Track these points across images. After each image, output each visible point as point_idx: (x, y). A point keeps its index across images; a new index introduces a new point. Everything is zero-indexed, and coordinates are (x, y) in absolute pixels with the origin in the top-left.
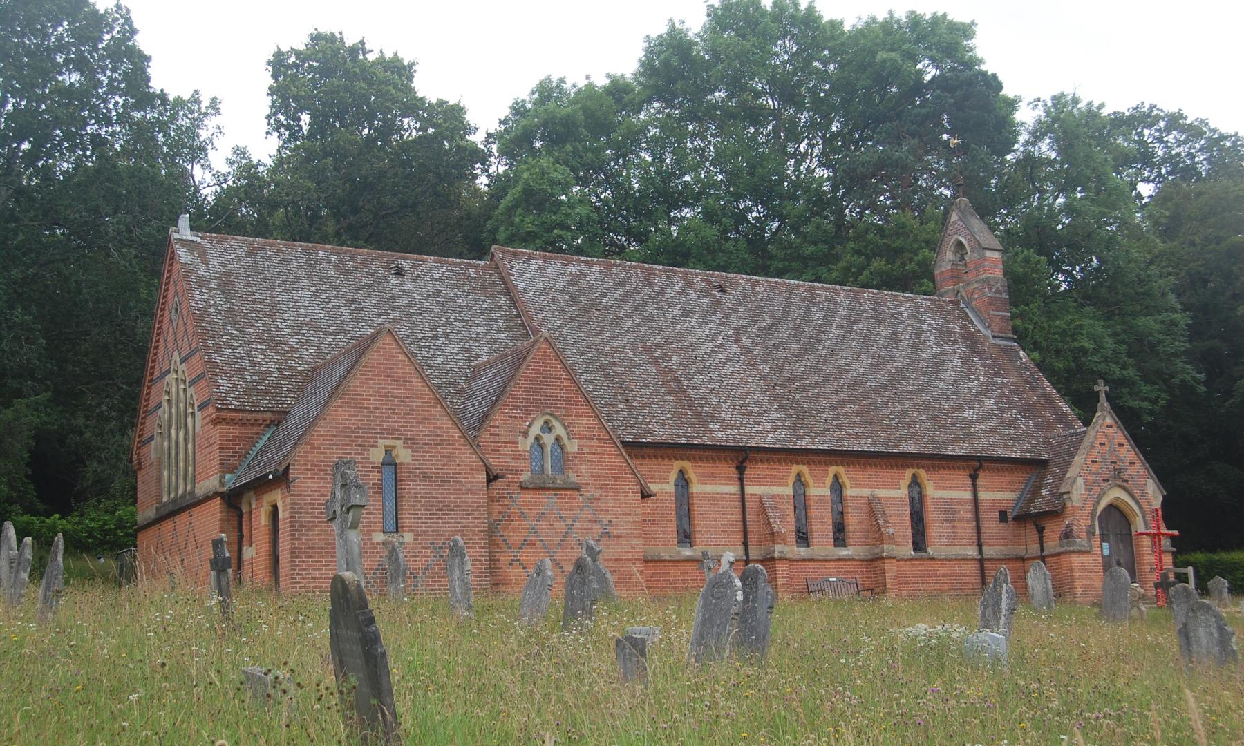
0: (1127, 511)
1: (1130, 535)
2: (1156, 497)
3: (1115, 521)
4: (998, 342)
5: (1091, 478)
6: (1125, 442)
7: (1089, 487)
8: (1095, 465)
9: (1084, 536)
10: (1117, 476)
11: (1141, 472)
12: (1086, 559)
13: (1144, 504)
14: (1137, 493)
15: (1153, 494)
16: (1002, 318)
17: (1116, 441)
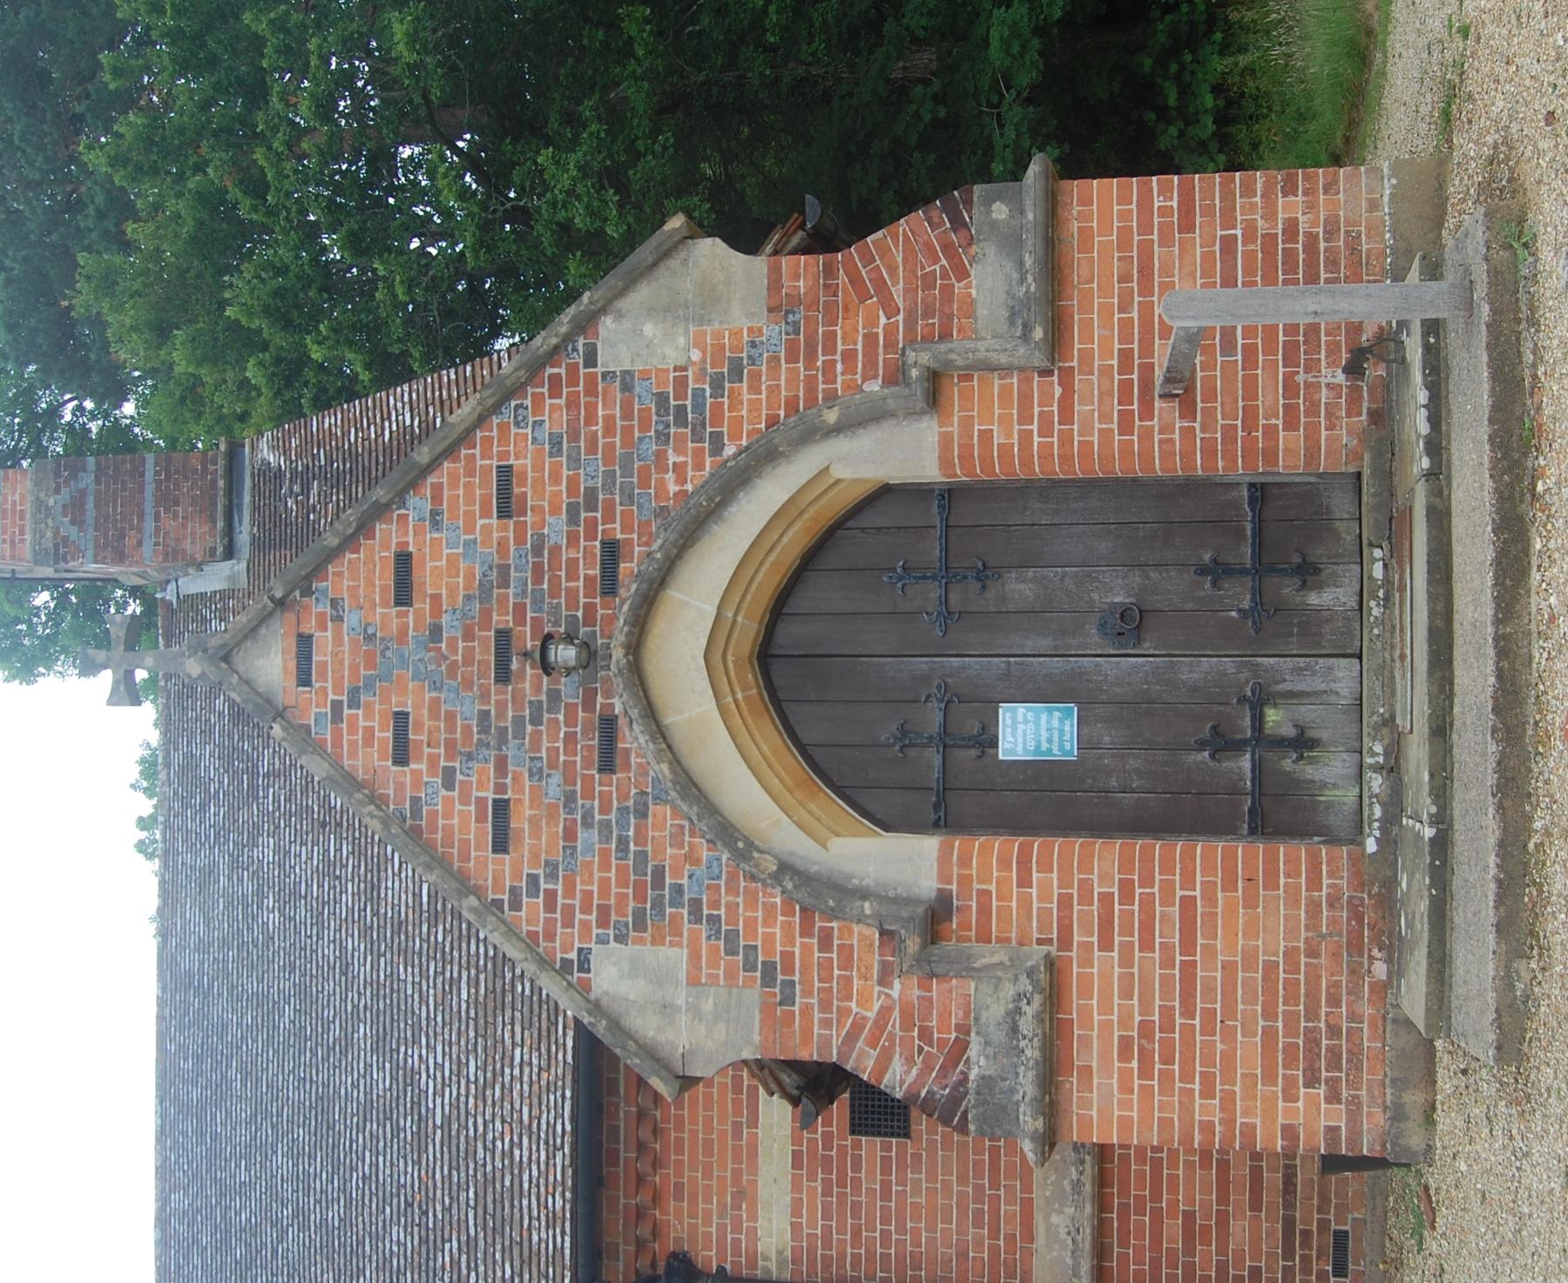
0: (795, 541)
1: (949, 495)
2: (710, 299)
3: (869, 648)
4: (244, 537)
5: (598, 876)
6: (388, 536)
7: (648, 907)
8: (521, 819)
9: (951, 995)
10: (577, 649)
11: (554, 415)
12: (1102, 1012)
13: (747, 412)
14: (683, 472)
15: (691, 311)
16: (167, 500)
17: (385, 615)
